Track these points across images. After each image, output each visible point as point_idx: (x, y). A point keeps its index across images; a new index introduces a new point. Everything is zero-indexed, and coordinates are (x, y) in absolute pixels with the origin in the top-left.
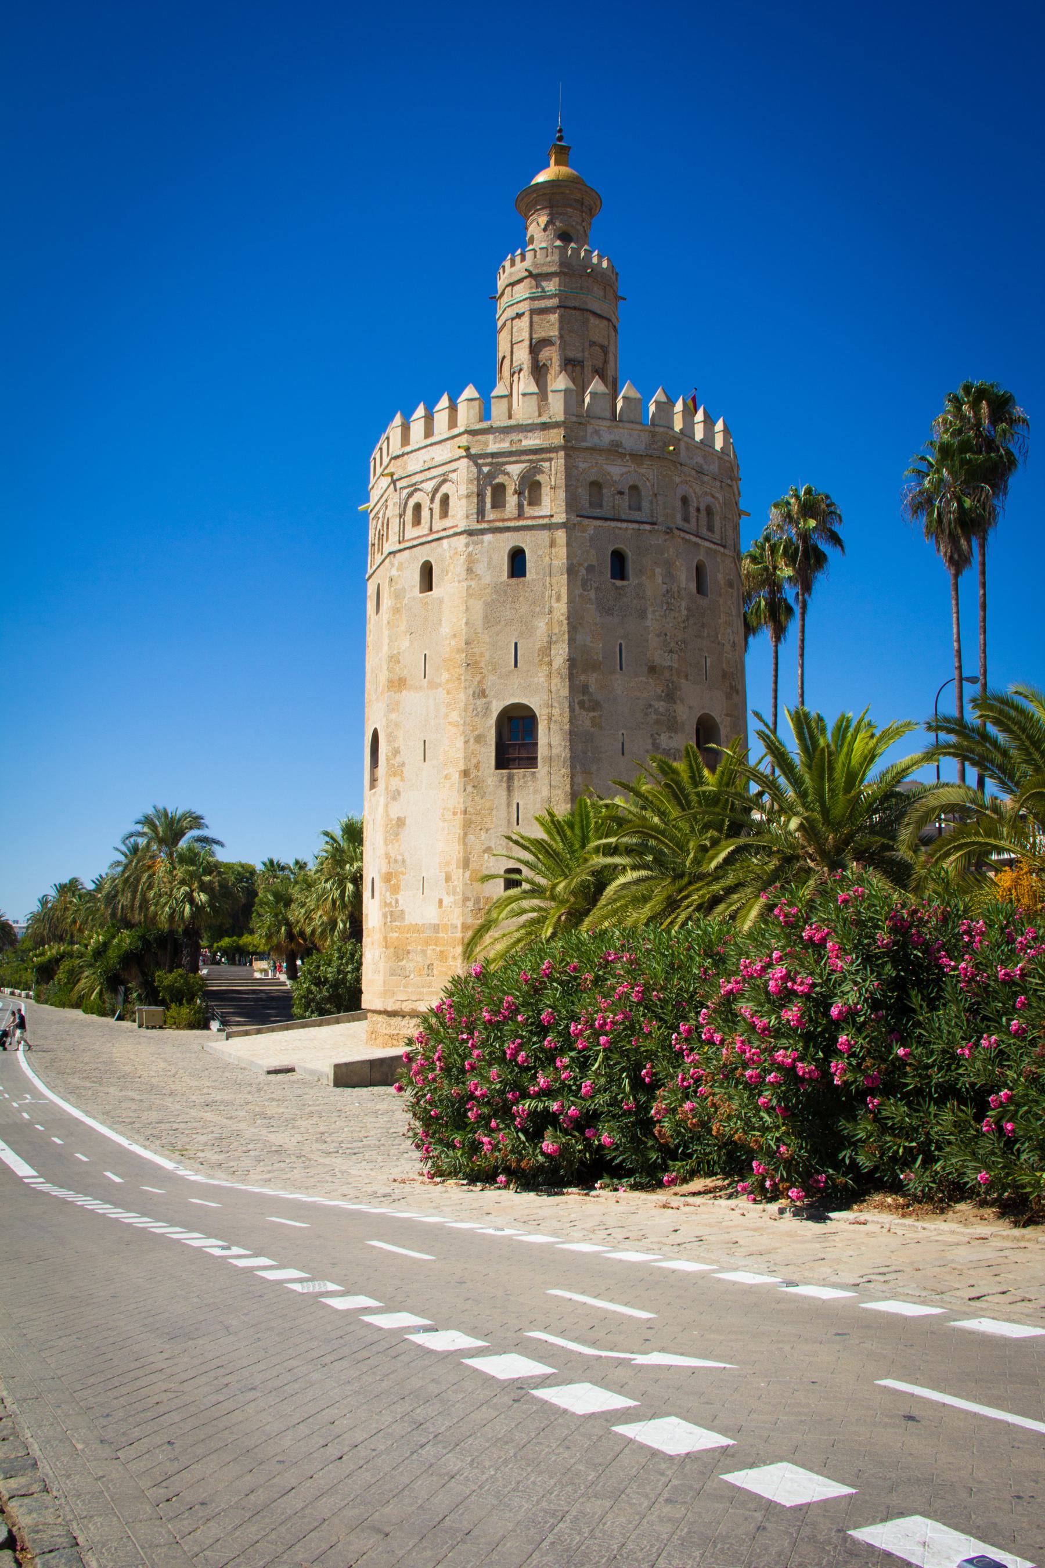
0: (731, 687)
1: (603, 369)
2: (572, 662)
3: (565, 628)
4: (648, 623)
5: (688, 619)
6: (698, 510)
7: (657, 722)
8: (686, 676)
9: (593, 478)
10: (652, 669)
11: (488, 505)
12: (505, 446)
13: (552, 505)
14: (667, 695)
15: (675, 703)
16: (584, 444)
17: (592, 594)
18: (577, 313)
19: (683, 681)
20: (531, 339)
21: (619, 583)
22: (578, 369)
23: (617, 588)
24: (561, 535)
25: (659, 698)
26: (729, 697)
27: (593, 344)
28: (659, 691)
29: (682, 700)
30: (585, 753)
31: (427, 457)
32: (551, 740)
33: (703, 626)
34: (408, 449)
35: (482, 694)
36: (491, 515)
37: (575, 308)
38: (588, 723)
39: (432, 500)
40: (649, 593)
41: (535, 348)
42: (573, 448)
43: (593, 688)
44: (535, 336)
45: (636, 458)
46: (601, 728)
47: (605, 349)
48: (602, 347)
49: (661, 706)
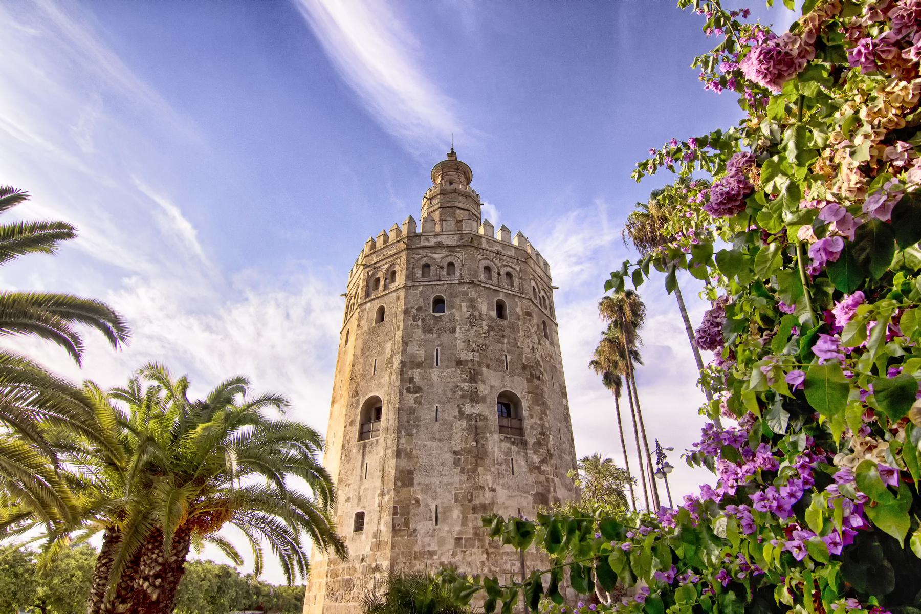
0: (531, 375)
2: (403, 364)
3: (400, 344)
4: (457, 335)
5: (488, 331)
6: (499, 274)
7: (462, 397)
8: (488, 367)
10: (459, 363)
12: (381, 257)
14: (470, 378)
15: (476, 382)
17: (419, 323)
19: (484, 370)
21: (437, 315)
23: (436, 317)
24: (402, 293)
25: (464, 381)
26: (529, 381)
28: (464, 376)
29: (483, 382)
30: (408, 422)
32: (388, 415)
33: (503, 336)
35: (356, 394)
38: (412, 401)
40: (458, 318)
43: (417, 379)
45: (451, 248)
46: (421, 404)
49: (465, 386)
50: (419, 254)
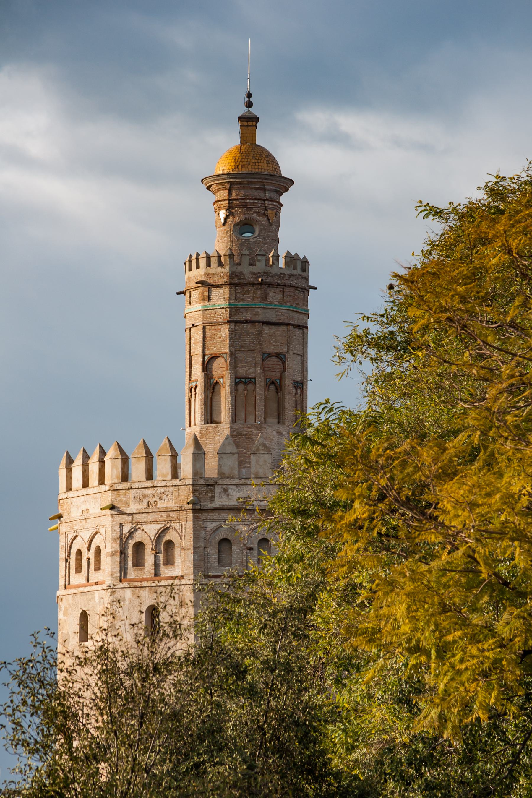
1: (280, 380)
9: (222, 536)
11: (130, 563)
13: (183, 564)
16: (212, 505)
18: (249, 326)
20: (204, 355)
22: (250, 387)
27: (270, 355)
31: (84, 507)
34: (70, 494)
36: (132, 574)
37: (246, 322)
39: (89, 550)
41: (207, 367)
42: (201, 510)
44: (207, 352)
47: (282, 358)
48: (278, 356)
50: (214, 520)
